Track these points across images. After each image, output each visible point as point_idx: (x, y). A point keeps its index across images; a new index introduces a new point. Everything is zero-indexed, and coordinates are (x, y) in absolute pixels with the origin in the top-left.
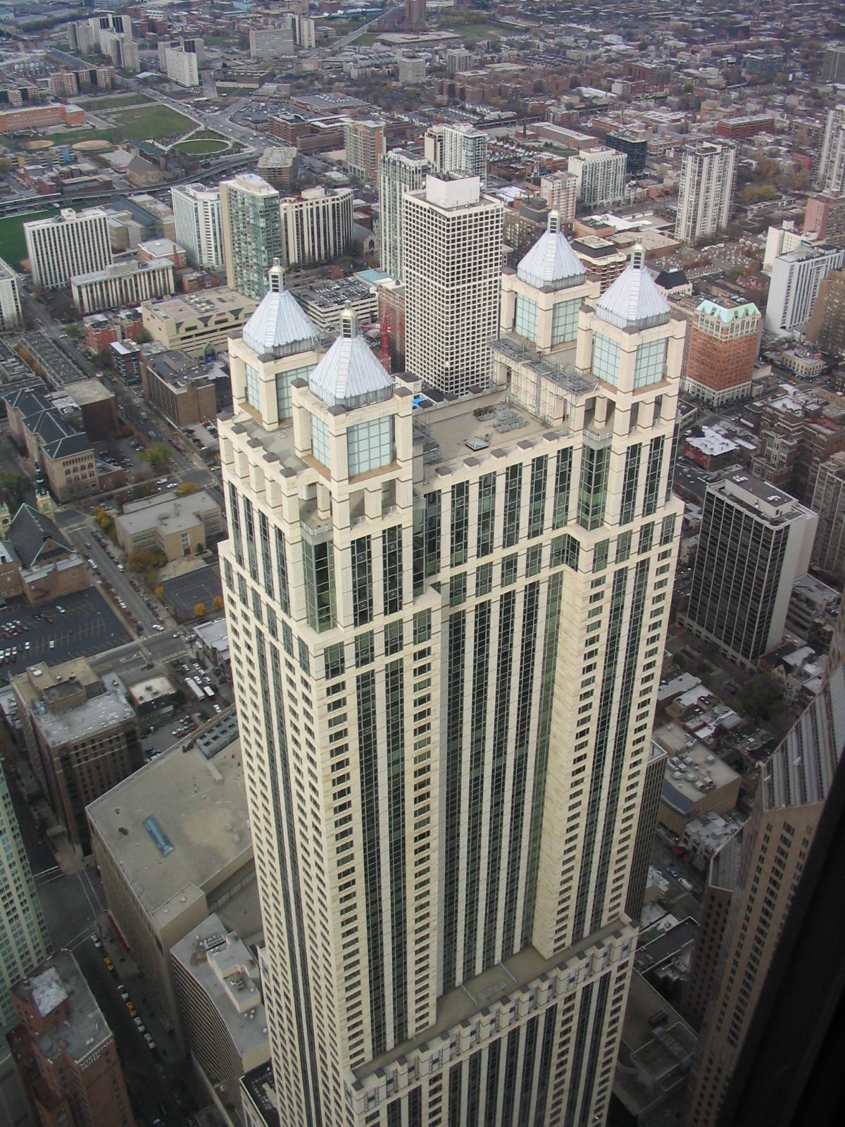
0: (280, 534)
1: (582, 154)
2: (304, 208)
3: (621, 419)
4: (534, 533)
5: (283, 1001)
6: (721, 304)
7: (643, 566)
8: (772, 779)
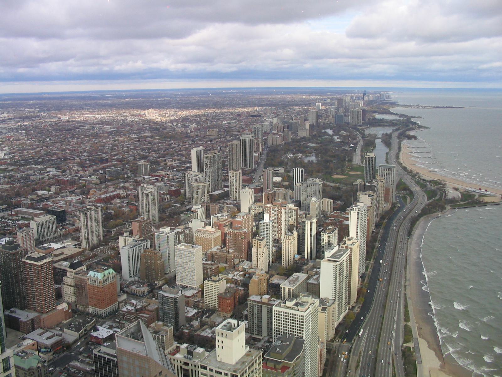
1: (36, 219)
6: (97, 271)
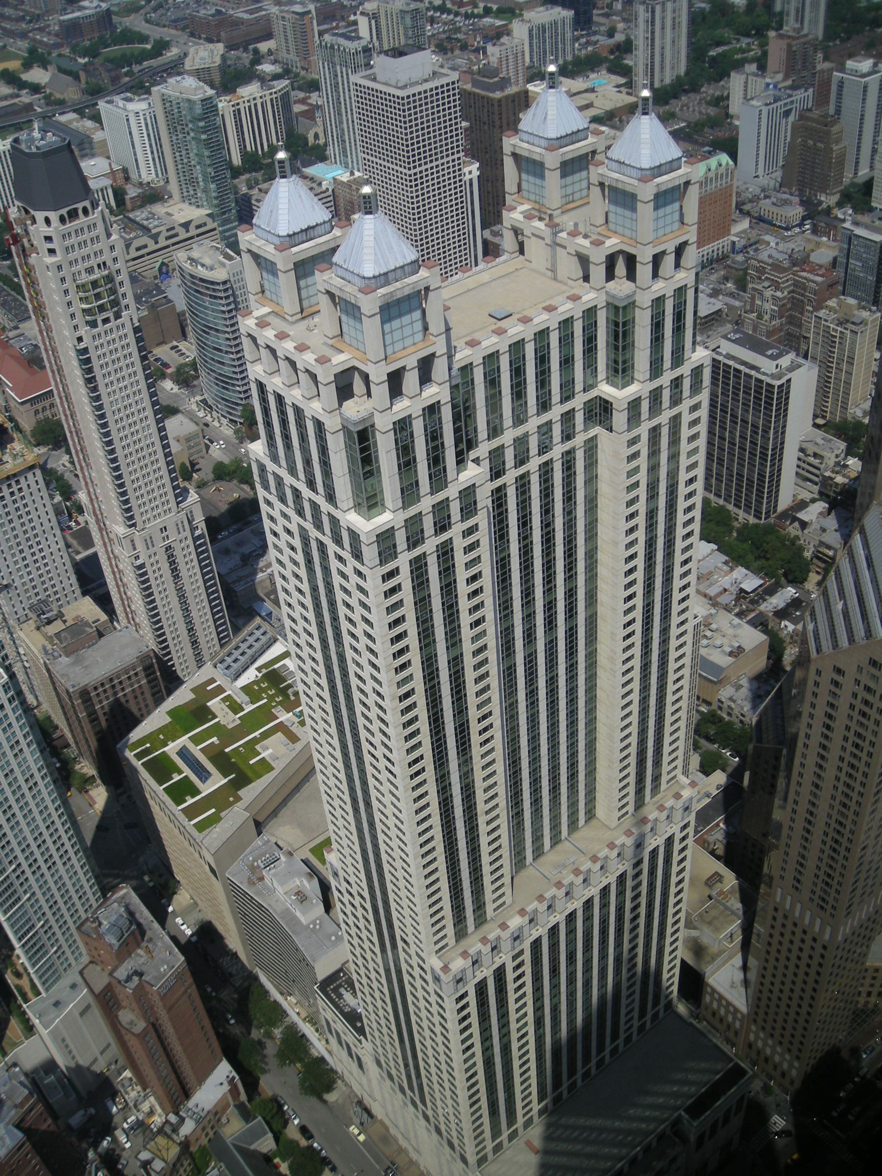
0: (319, 426)
2: (241, 107)
3: (644, 271)
4: (565, 399)
5: (357, 901)
7: (676, 421)
8: (816, 626)
